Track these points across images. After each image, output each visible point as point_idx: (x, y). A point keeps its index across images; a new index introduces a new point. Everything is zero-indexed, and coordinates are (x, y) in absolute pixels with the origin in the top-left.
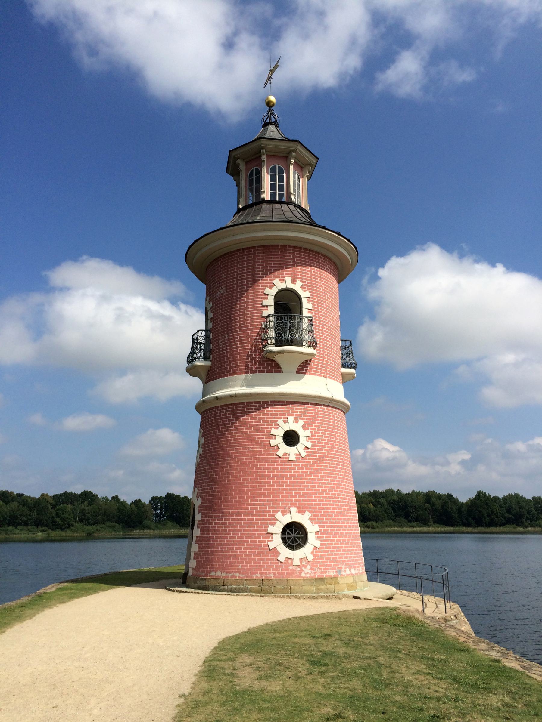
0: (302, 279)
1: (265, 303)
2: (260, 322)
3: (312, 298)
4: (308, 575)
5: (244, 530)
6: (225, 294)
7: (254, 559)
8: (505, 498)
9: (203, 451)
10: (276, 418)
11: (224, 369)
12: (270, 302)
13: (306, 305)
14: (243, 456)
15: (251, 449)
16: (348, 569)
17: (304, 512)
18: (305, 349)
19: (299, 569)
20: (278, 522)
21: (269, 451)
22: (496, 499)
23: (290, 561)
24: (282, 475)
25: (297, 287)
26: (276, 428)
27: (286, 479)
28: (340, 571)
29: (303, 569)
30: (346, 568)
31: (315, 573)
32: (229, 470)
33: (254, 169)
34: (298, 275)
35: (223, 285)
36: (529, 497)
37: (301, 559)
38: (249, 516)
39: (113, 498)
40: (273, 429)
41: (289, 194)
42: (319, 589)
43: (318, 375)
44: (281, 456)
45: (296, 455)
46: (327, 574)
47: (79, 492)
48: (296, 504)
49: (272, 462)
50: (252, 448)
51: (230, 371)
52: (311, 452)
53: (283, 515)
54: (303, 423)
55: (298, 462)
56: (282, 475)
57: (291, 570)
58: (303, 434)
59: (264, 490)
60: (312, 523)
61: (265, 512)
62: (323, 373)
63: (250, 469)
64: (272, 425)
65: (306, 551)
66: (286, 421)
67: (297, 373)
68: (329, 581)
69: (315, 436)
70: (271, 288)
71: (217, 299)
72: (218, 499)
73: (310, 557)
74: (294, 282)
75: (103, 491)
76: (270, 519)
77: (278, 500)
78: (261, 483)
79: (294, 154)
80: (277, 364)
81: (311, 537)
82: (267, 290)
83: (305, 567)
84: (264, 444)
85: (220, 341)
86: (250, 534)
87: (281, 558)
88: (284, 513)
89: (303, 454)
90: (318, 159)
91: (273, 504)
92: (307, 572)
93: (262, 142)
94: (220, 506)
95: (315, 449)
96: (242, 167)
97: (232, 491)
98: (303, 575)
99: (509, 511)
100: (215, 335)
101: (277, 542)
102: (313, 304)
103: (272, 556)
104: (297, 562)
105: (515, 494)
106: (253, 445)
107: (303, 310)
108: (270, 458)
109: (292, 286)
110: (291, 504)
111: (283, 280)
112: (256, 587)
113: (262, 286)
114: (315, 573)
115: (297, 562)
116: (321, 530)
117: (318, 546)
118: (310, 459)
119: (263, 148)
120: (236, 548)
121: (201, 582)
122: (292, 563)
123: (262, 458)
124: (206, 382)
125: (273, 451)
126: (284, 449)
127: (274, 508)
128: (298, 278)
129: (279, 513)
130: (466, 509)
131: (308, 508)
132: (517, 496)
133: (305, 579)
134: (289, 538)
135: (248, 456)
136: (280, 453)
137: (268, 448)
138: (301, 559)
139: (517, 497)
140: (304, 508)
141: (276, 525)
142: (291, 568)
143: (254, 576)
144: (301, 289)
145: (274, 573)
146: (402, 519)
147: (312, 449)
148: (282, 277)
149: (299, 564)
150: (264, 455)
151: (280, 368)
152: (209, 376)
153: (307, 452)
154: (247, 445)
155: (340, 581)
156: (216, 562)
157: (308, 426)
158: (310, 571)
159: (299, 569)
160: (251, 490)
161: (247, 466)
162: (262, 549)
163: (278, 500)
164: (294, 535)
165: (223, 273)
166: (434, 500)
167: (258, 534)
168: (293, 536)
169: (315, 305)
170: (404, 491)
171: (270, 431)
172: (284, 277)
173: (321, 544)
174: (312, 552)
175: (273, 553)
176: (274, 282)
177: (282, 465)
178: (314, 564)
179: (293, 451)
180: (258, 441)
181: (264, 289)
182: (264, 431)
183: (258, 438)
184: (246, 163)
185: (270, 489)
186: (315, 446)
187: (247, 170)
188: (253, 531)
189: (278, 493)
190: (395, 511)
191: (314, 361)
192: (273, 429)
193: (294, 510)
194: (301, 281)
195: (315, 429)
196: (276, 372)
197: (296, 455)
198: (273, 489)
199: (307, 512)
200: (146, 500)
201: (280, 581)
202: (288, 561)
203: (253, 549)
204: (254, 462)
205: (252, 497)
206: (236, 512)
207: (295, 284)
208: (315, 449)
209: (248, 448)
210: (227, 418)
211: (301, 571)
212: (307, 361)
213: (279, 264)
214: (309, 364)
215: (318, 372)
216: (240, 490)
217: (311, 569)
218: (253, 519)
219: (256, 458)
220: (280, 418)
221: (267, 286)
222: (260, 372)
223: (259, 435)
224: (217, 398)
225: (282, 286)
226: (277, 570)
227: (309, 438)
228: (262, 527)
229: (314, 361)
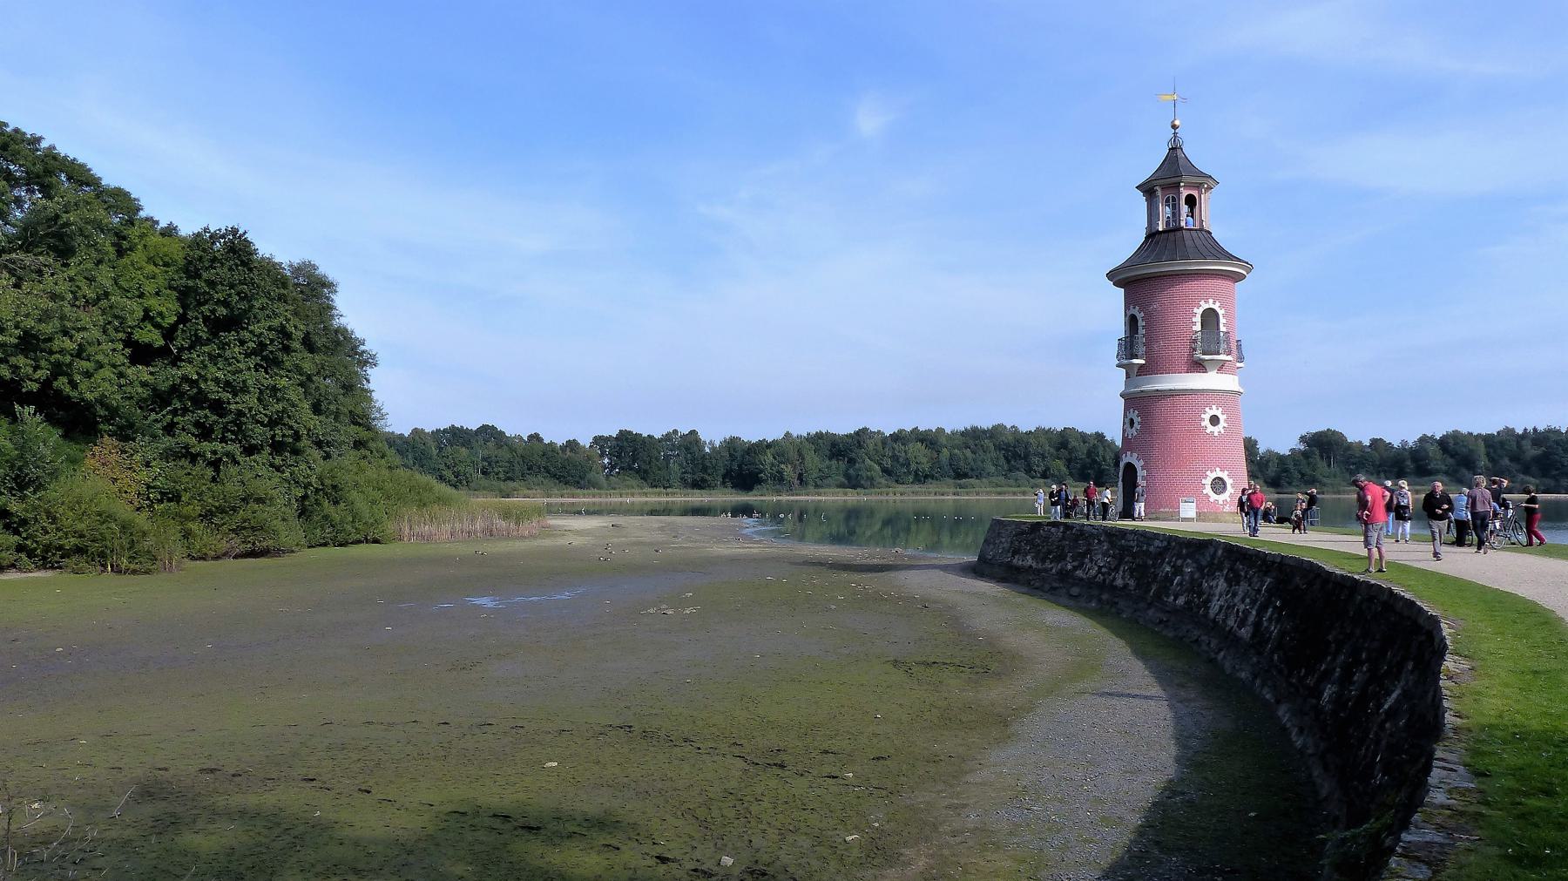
12: (1198, 319)
13: (1222, 321)
25: (1216, 307)
39: (531, 437)
47: (474, 426)
58: (1222, 418)
75: (515, 426)
92: (1227, 509)
96: (1159, 193)
126: (1210, 428)
166: (1073, 443)
170: (1023, 428)
179: (1216, 430)
190: (1008, 461)
200: (585, 441)
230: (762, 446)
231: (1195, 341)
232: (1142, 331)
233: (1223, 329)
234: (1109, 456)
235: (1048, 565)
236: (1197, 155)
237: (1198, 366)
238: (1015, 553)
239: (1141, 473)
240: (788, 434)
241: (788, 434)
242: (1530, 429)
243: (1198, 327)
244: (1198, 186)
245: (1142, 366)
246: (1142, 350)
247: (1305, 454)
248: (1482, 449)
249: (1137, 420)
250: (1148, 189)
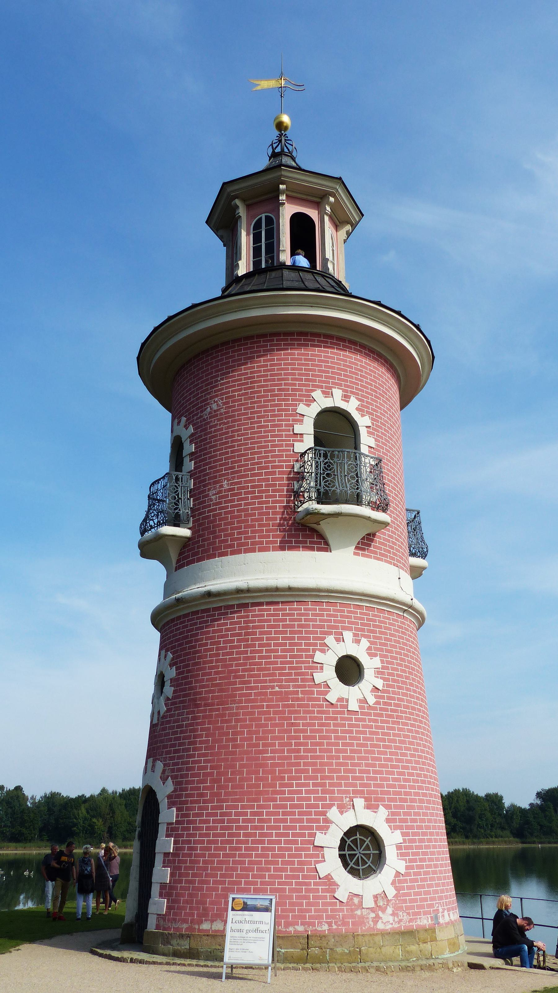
0: (358, 394)
1: (298, 429)
2: (290, 461)
3: (373, 429)
4: (389, 927)
5: (270, 842)
6: (223, 411)
7: (291, 897)
9: (175, 692)
10: (321, 633)
11: (220, 542)
12: (307, 428)
13: (366, 441)
14: (262, 701)
15: (277, 689)
16: (446, 913)
17: (377, 807)
19: (373, 915)
20: (333, 827)
21: (312, 693)
23: (356, 900)
24: (337, 738)
26: (323, 651)
27: (344, 744)
28: (437, 918)
29: (380, 913)
30: (444, 910)
31: (400, 921)
32: (235, 727)
33: (263, 216)
34: (352, 388)
35: (217, 396)
36: (482, 793)
37: (376, 897)
38: (278, 814)
40: (317, 653)
41: (325, 261)
42: (408, 952)
43: (386, 561)
44: (334, 702)
45: (360, 701)
46: (419, 922)
48: (362, 792)
49: (319, 712)
50: (280, 687)
51: (232, 546)
52: (383, 697)
53: (342, 813)
54: (368, 644)
55: (362, 714)
56: (321, 738)
57: (359, 917)
58: (370, 665)
59: (305, 764)
60: (390, 826)
61: (308, 806)
62: (393, 559)
63: (276, 725)
64: (316, 645)
65: (382, 882)
66: (340, 639)
67: (355, 554)
68: (422, 935)
69: (387, 668)
70: (308, 405)
71: (204, 420)
72: (213, 781)
73: (391, 893)
74: (346, 398)
76: (318, 821)
77: (331, 785)
78: (299, 751)
79: (332, 199)
80: (321, 536)
81: (390, 853)
82: (302, 408)
83: (384, 910)
84: (303, 680)
85: (211, 493)
86: (280, 849)
87: (342, 894)
88: (342, 809)
89: (371, 700)
90: (363, 215)
91: (323, 792)
92: (387, 921)
93: (283, 173)
94: (218, 794)
95: (388, 692)
96: (242, 212)
97: (242, 766)
98: (380, 926)
100: (200, 482)
101: (331, 865)
102: (376, 440)
103: (323, 891)
104: (369, 902)
105: (463, 789)
106: (281, 680)
107: (362, 447)
108: (313, 706)
109: (343, 405)
110: (354, 792)
111: (328, 394)
112: (296, 951)
113: (292, 400)
114: (400, 921)
115: (369, 902)
116: (405, 841)
117: (403, 871)
118: (381, 709)
119: (283, 184)
120: (254, 876)
121: (182, 942)
122: (361, 903)
123: (299, 706)
124: (179, 567)
125: (319, 693)
126: (338, 690)
127: (325, 799)
128: (352, 393)
129: (334, 809)
131: (383, 800)
133: (384, 934)
134: (352, 856)
135: (272, 700)
136: (332, 697)
137: (310, 686)
138: (376, 897)
140: (376, 800)
141: (330, 830)
142: (358, 912)
143: (291, 929)
144: (357, 412)
145: (330, 924)
147: (383, 691)
148: (326, 387)
149: (372, 905)
150: (302, 699)
151: (327, 543)
152: (183, 557)
153: (376, 697)
154: (270, 681)
155: (441, 935)
156: (212, 903)
157: (376, 649)
158: (391, 919)
159: (373, 915)
160: (278, 765)
161: (271, 719)
162: (304, 877)
163: (331, 785)
164: (362, 850)
165: (217, 376)
167: (297, 849)
168: (359, 852)
169: (379, 441)
171: (312, 656)
172: (330, 388)
173: (407, 868)
174: (393, 883)
175: (324, 884)
176: (313, 394)
177: (336, 719)
178: (401, 903)
180: (290, 674)
181: (296, 405)
182: (301, 657)
183: (290, 668)
184: (249, 207)
185: (315, 764)
186: (388, 686)
187: (250, 218)
188: (286, 842)
189: (330, 771)
191: (380, 538)
192: (317, 653)
193: (359, 802)
194: (357, 398)
195: (386, 656)
196: (319, 550)
197: (360, 701)
198: (322, 764)
199: (381, 808)
201: (341, 938)
202: (352, 899)
203: (287, 877)
204: (283, 712)
205: (283, 778)
206: (252, 807)
207: (348, 402)
208: (388, 692)
209: (273, 687)
210: (227, 630)
211: (377, 919)
212: (369, 535)
213: (321, 366)
214: (372, 541)
215: (386, 556)
216: (258, 766)
217: (393, 914)
218: (285, 821)
219: (288, 706)
220: (330, 633)
221: (302, 401)
222: (291, 548)
223: (292, 663)
224: (209, 594)
225: (328, 403)
226: (333, 917)
227: (379, 673)
228: (303, 835)
229: (380, 538)
230: (81, 800)
231: (300, 477)
232: (189, 465)
237: (306, 533)
240: (104, 791)
241: (104, 791)
244: (317, 199)
247: (540, 807)
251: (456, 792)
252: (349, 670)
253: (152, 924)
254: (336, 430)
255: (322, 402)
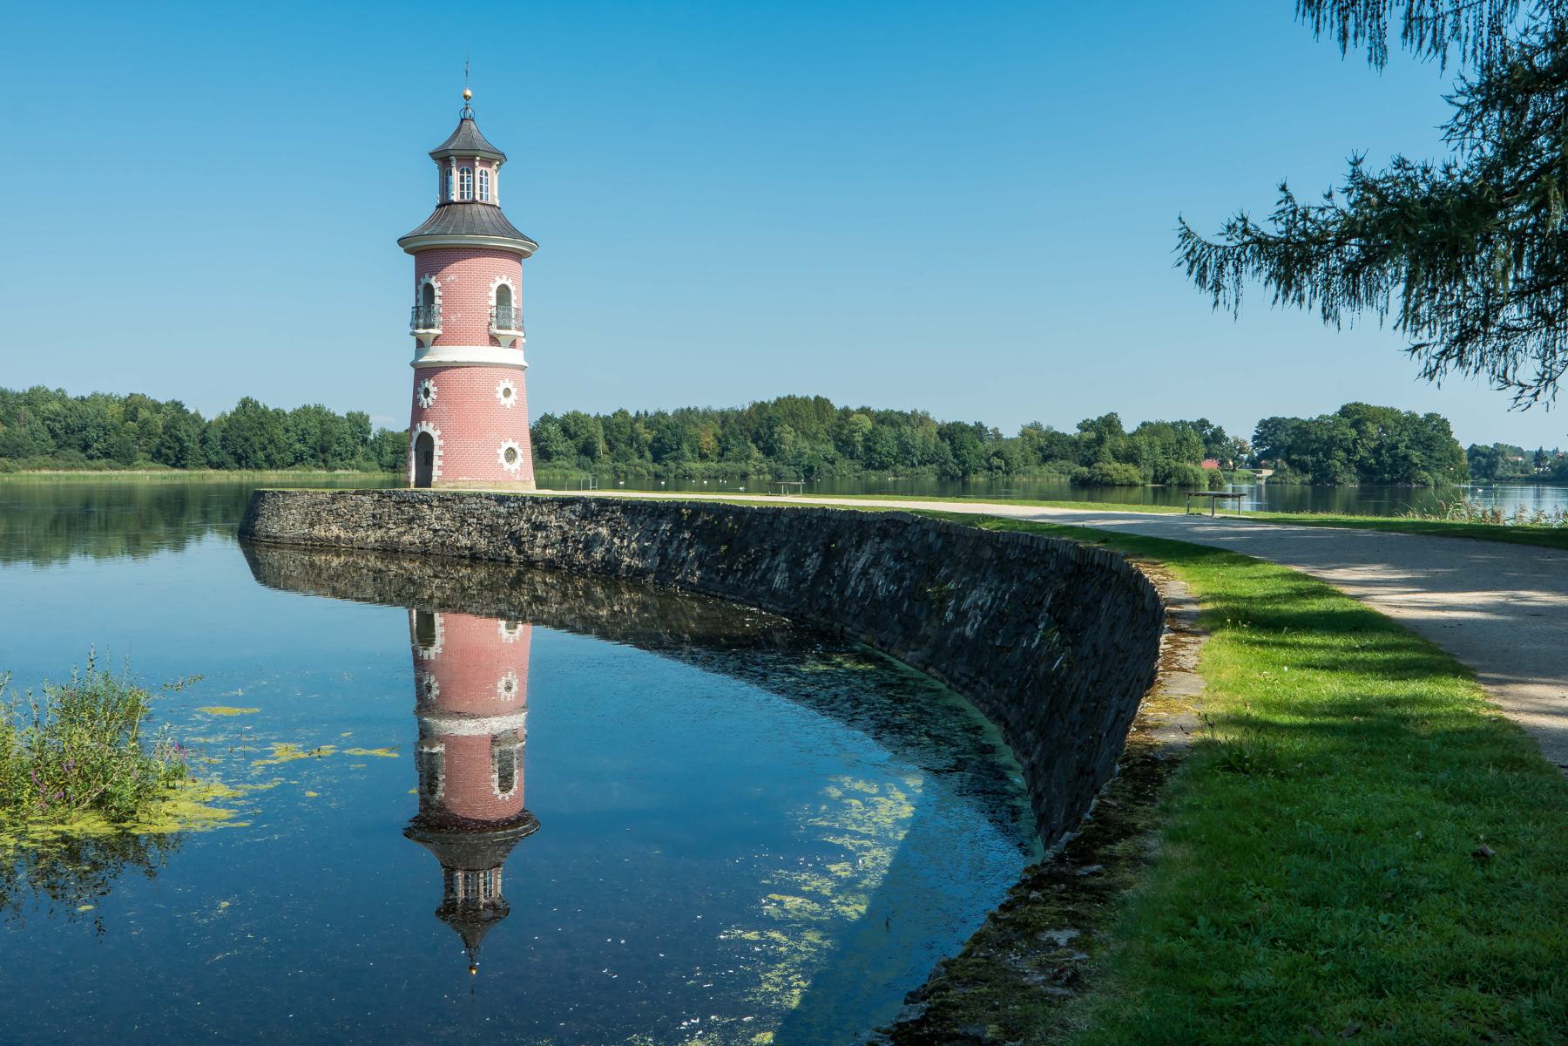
8: (296, 414)
12: (493, 294)
13: (514, 297)
18: (513, 332)
22: (279, 414)
25: (509, 283)
36: (341, 412)
99: (302, 440)
101: (502, 459)
126: (504, 401)
130: (220, 435)
132: (319, 410)
139: (319, 413)
146: (74, 453)
179: (508, 402)
233: (514, 305)
234: (195, 431)
235: (361, 533)
236: (486, 131)
238: (312, 525)
239: (437, 442)
242: (642, 412)
243: (493, 302)
245: (438, 337)
246: (438, 319)
248: (601, 431)
249: (433, 389)
250: (443, 159)
251: (306, 409)
252: (507, 392)
253: (435, 479)
254: (503, 293)
255: (499, 282)
